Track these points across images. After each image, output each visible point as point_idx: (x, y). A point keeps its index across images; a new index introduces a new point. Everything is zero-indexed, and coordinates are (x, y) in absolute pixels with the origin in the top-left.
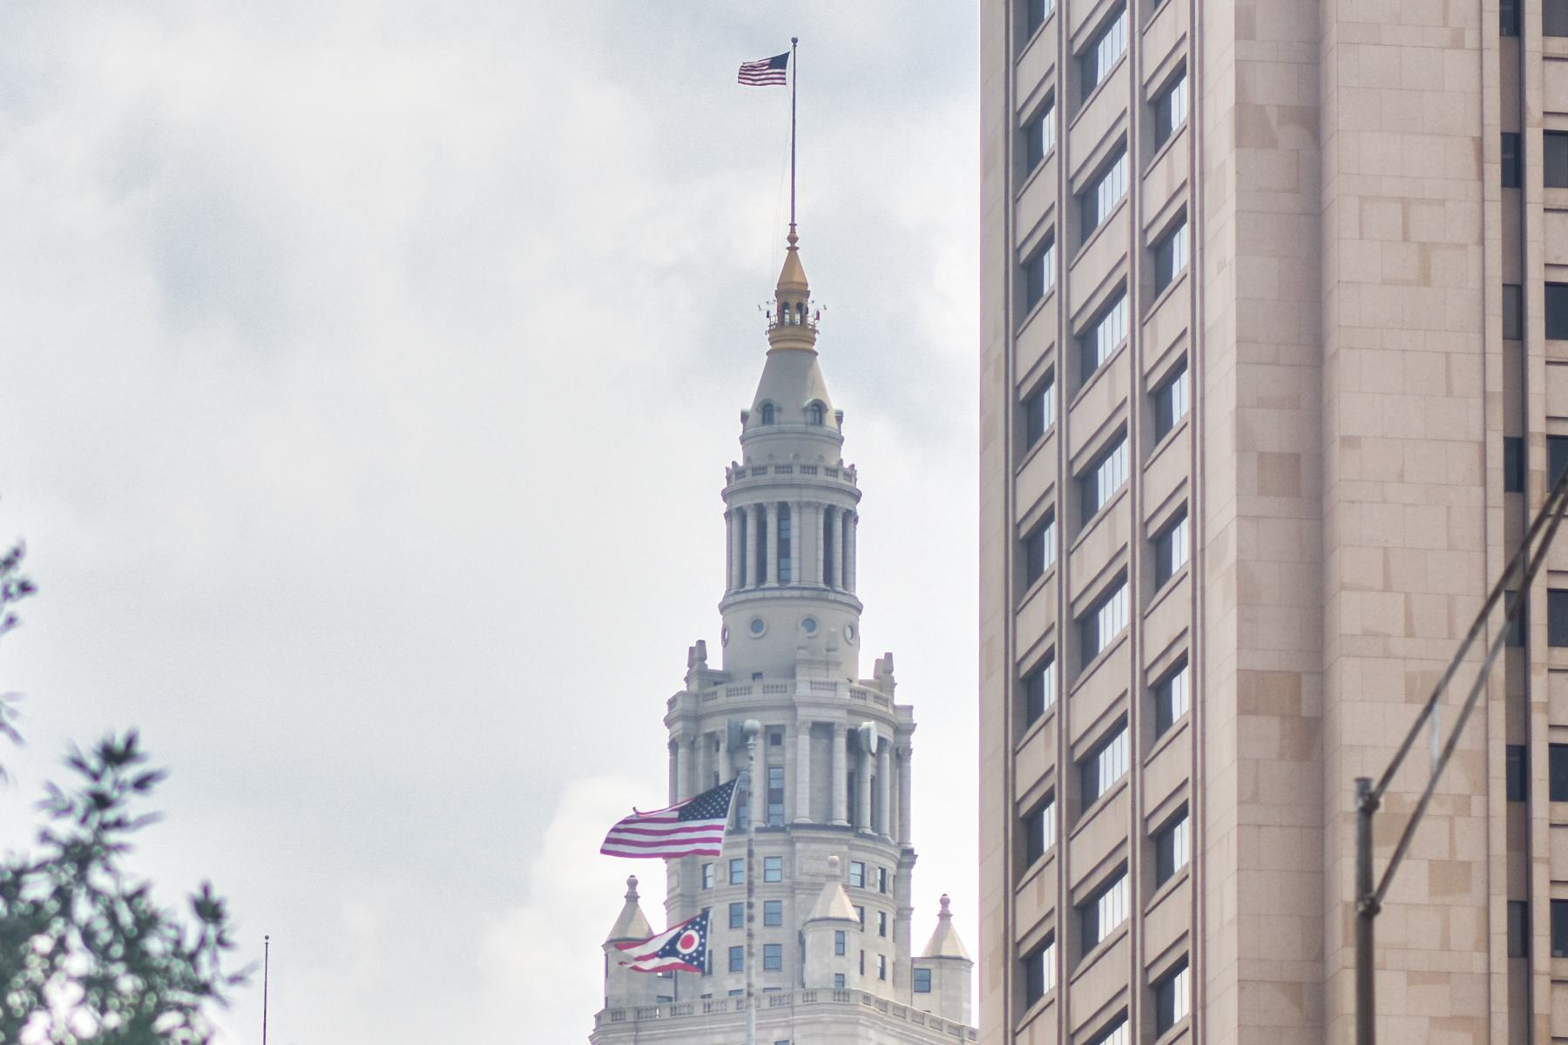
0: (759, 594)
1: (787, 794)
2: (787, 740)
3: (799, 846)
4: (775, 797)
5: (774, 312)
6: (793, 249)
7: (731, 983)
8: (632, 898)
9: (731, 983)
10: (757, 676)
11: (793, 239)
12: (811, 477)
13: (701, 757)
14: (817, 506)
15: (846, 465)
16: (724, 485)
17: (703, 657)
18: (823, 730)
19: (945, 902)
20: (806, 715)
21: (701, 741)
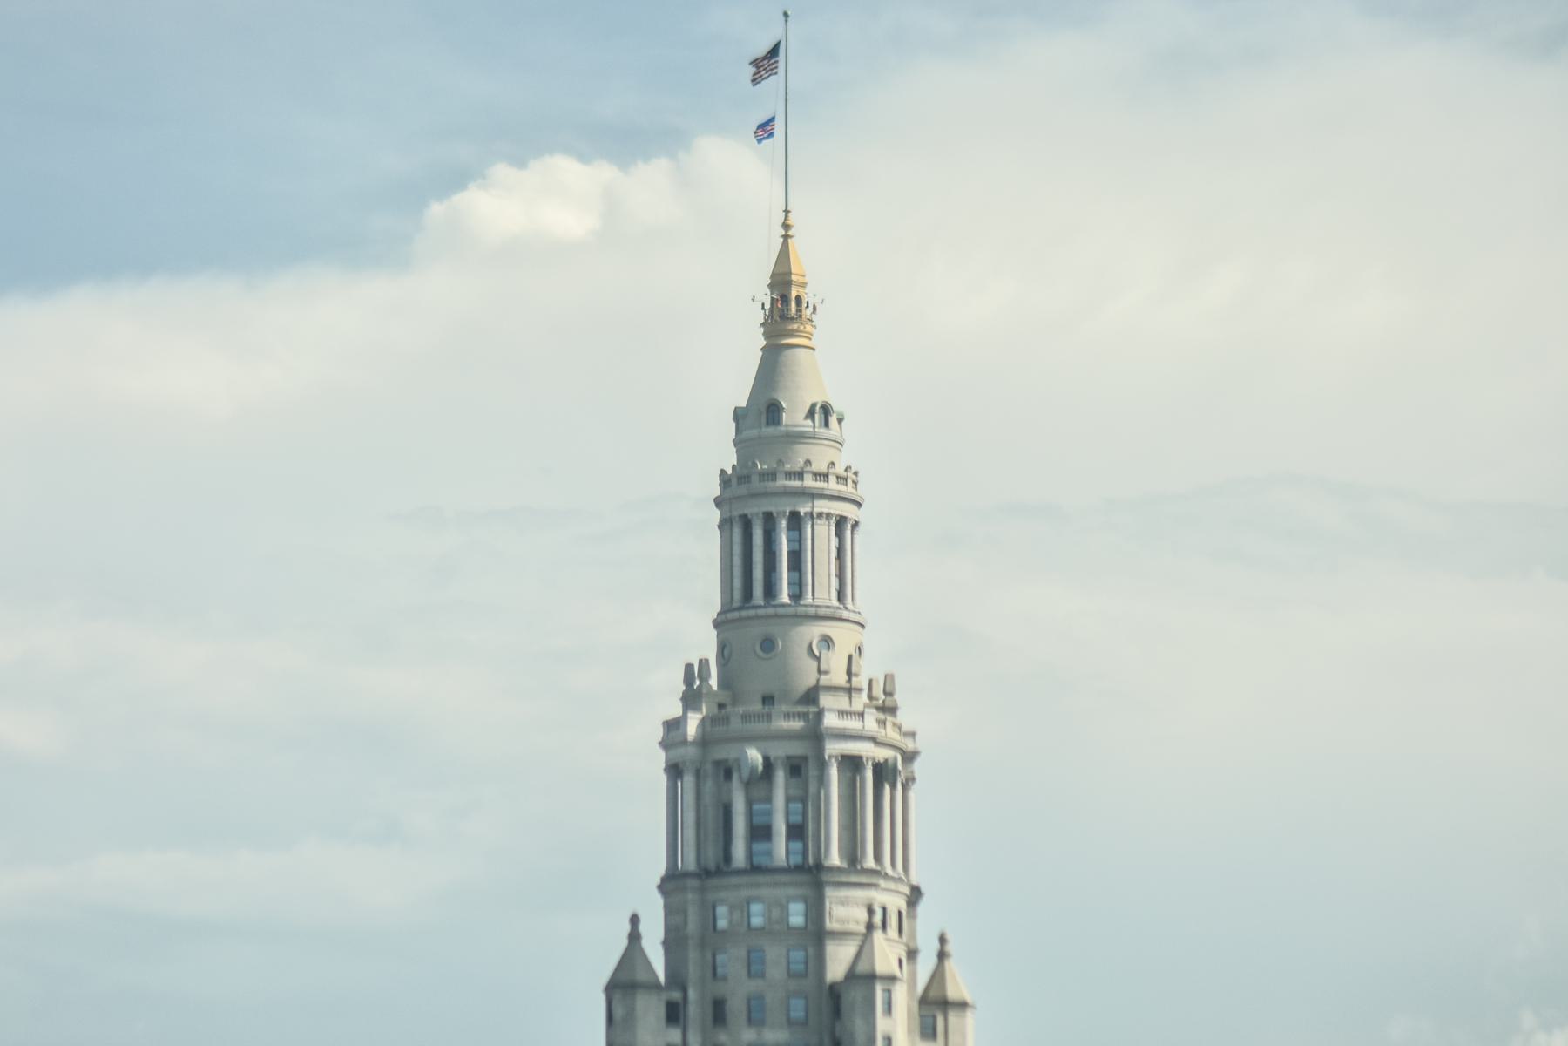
0: (770, 611)
2: (812, 772)
4: (796, 832)
5: (768, 306)
8: (634, 937)
11: (786, 226)
12: (822, 485)
13: (709, 786)
14: (829, 516)
17: (704, 676)
18: (852, 764)
19: (942, 940)
21: (709, 767)
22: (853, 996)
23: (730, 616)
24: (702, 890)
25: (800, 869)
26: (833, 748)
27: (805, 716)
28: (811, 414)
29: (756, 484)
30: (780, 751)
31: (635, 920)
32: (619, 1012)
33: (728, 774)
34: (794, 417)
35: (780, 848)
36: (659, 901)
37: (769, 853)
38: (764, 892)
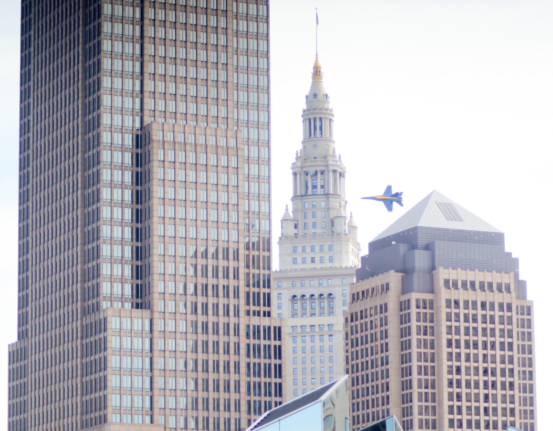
1: (326, 186)
2: (326, 173)
3: (330, 199)
6: (317, 58)
8: (287, 210)
9: (313, 231)
10: (315, 158)
11: (317, 55)
13: (303, 177)
14: (328, 118)
15: (330, 108)
16: (302, 114)
18: (334, 171)
19: (351, 213)
20: (331, 168)
21: (303, 173)
22: (336, 222)
24: (301, 199)
25: (324, 195)
26: (331, 168)
27: (324, 161)
28: (324, 96)
29: (312, 111)
30: (319, 169)
31: (287, 206)
33: (307, 174)
34: (320, 97)
35: (319, 191)
36: (291, 202)
37: (317, 192)
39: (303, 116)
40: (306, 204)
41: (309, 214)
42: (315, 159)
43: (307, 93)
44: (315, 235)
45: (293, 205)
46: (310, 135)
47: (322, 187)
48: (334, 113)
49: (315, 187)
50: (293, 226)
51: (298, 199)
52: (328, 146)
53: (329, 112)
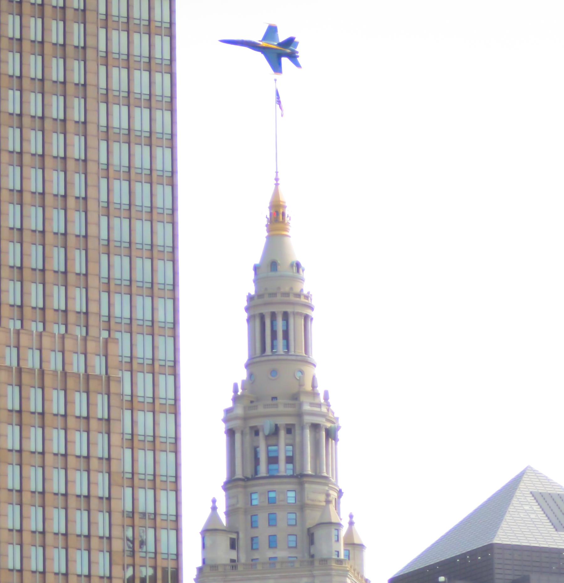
1: (297, 458)
2: (297, 431)
3: (307, 486)
5: (269, 217)
6: (277, 185)
7: (270, 554)
8: (214, 508)
9: (270, 554)
10: (274, 398)
11: (277, 179)
12: (298, 299)
13: (248, 438)
14: (300, 314)
16: (245, 304)
18: (315, 427)
19: (351, 516)
20: (308, 419)
21: (247, 430)
22: (319, 534)
23: (255, 360)
24: (245, 487)
25: (292, 477)
26: (308, 419)
27: (293, 406)
28: (292, 265)
29: (267, 299)
30: (282, 421)
31: (214, 501)
32: (208, 543)
33: (257, 433)
34: (283, 269)
35: (283, 468)
36: (223, 493)
37: (278, 470)
38: (276, 487)
39: (247, 309)
40: (255, 496)
41: (262, 519)
42: (275, 402)
43: (258, 261)
44: (274, 564)
45: (228, 498)
46: (263, 349)
47: (290, 460)
48: (314, 302)
49: (273, 460)
50: (228, 543)
51: (237, 487)
52: (302, 372)
53: (303, 299)
